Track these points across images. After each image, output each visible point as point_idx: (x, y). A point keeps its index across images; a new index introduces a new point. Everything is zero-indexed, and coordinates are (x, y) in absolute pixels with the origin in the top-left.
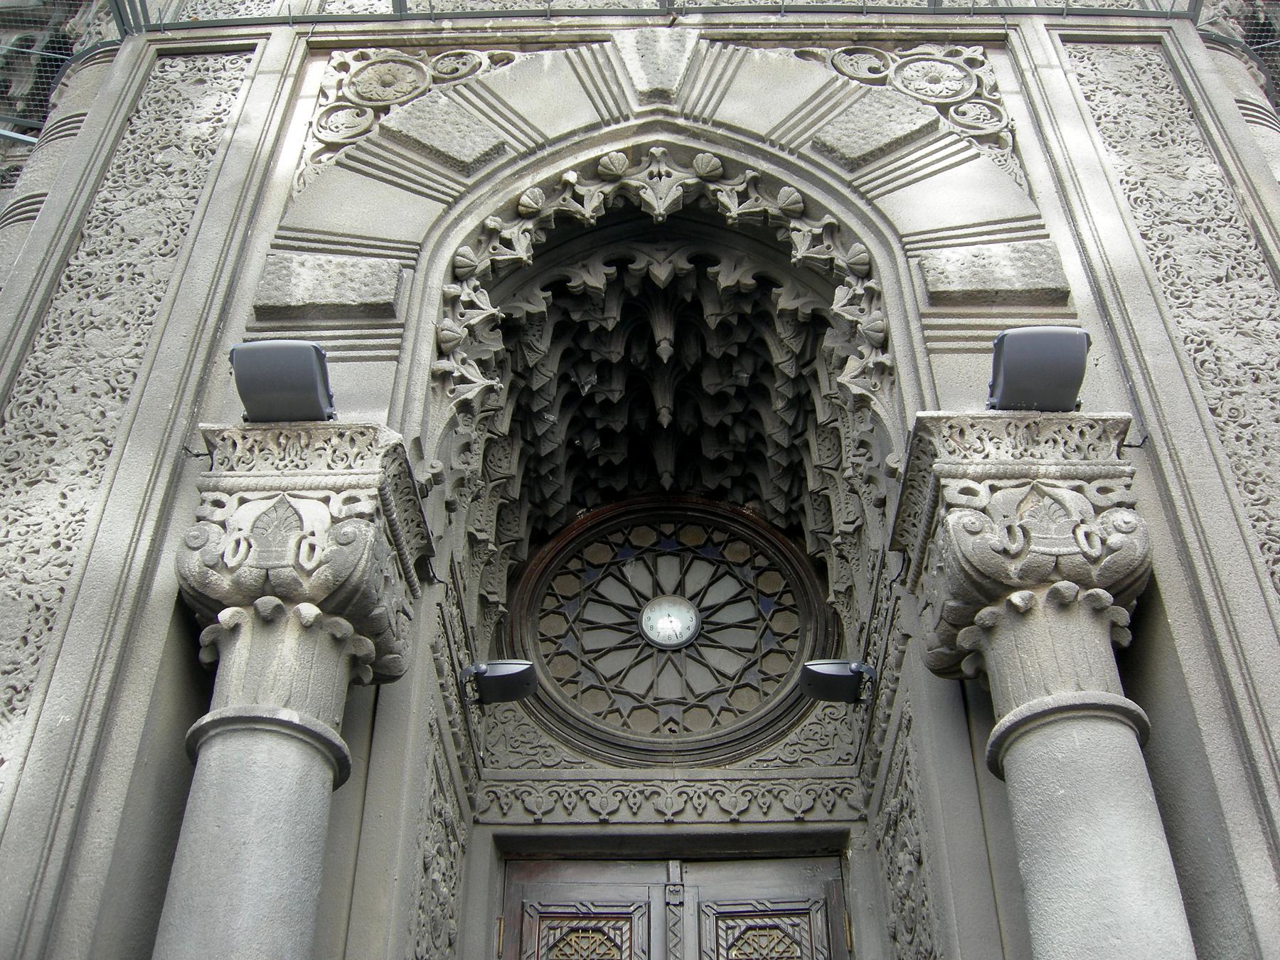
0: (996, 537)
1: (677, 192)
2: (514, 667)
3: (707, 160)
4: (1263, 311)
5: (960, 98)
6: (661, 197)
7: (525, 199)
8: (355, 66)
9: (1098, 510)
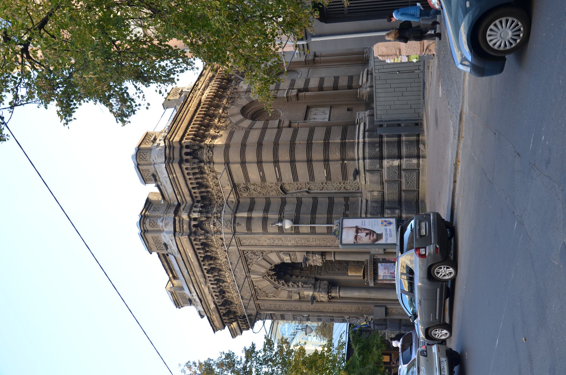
6: (273, 273)
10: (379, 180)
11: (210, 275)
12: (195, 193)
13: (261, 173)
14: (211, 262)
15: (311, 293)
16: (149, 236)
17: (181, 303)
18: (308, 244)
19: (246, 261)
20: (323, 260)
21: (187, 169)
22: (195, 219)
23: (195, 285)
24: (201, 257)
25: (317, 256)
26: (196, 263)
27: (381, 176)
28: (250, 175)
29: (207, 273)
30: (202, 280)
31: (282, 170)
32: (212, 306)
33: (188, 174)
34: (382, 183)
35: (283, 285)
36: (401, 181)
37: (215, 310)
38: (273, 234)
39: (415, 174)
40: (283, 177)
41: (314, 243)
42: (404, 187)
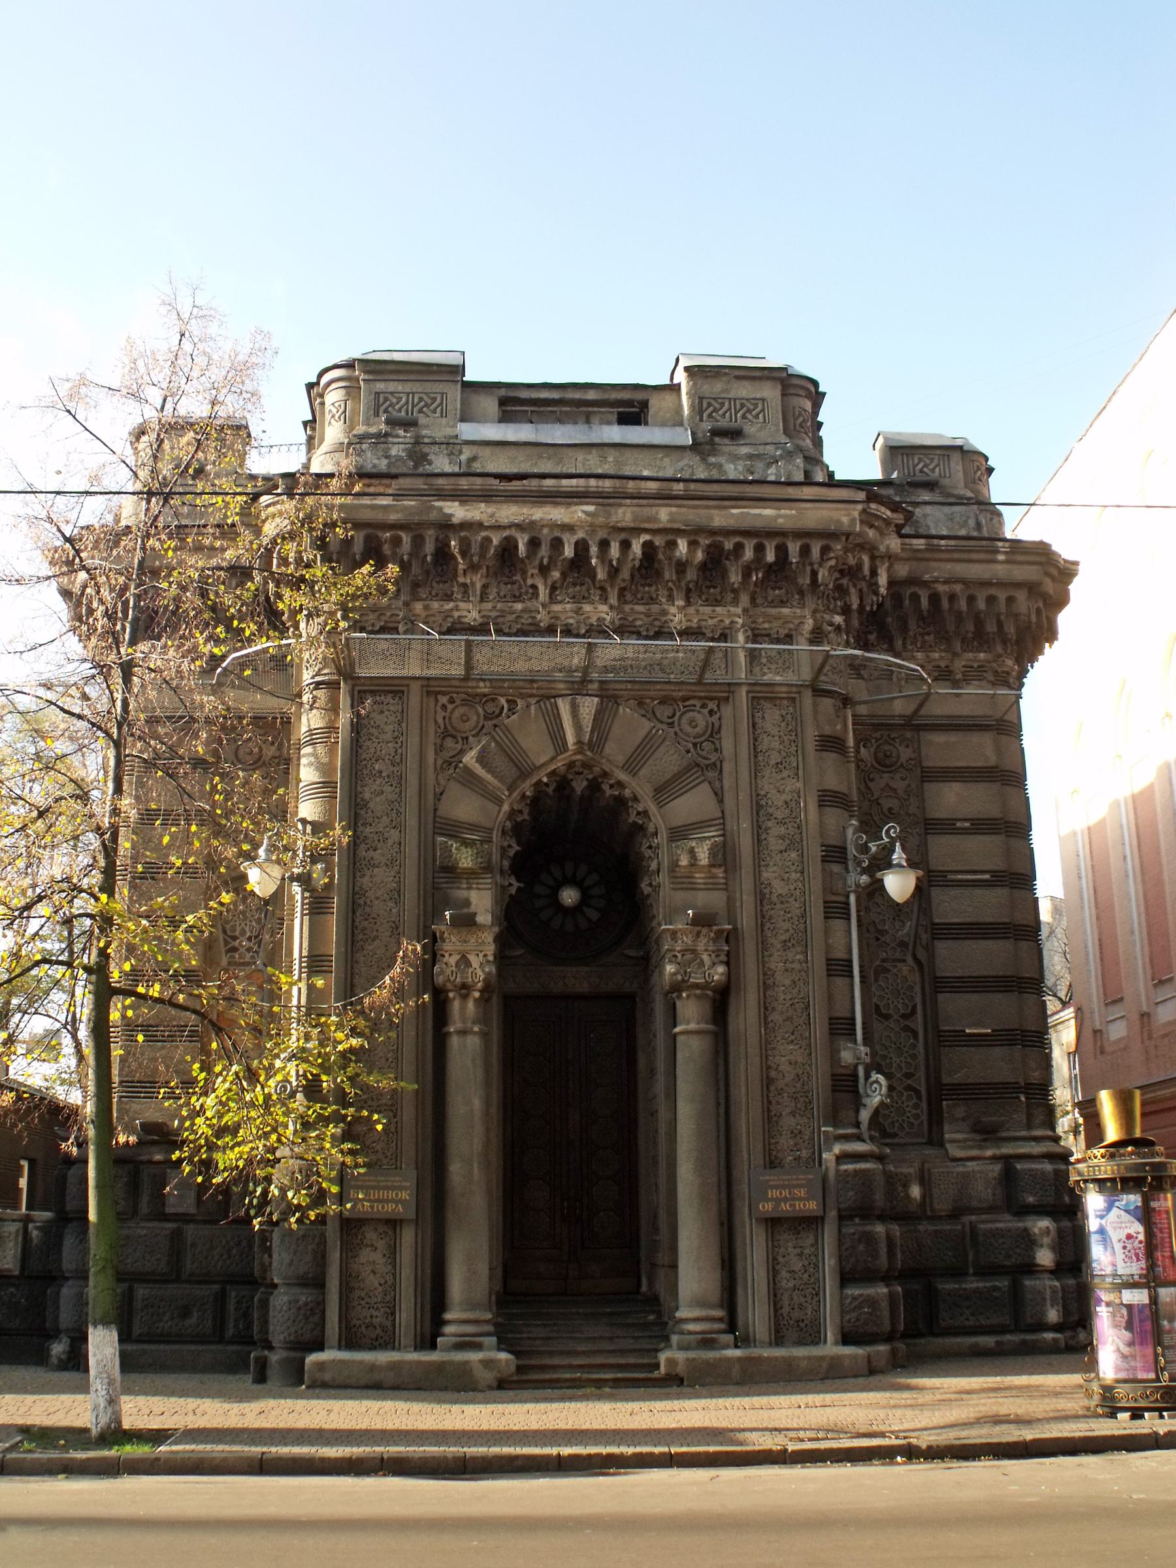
0: (679, 977)
1: (585, 783)
2: (519, 952)
3: (597, 770)
4: (793, 868)
5: (703, 739)
6: (579, 785)
7: (528, 793)
8: (450, 707)
9: (714, 964)
10: (975, 1203)
11: (637, 548)
12: (915, 598)
13: (967, 824)
14: (691, 575)
15: (484, 918)
16: (771, 393)
17: (380, 386)
18: (775, 942)
19: (663, 701)
20: (697, 986)
21: (1010, 600)
22: (874, 573)
23: (608, 483)
24: (739, 547)
25: (721, 969)
26: (719, 518)
27: (991, 1209)
28: (956, 786)
29: (646, 545)
30: (624, 515)
31: (979, 892)
32: (457, 512)
33: (991, 600)
34: (956, 1214)
35: (512, 814)
36: (967, 1274)
37: (433, 516)
38: (821, 824)
39: (1006, 1320)
40: (955, 892)
41: (775, 963)
42: (947, 1286)
